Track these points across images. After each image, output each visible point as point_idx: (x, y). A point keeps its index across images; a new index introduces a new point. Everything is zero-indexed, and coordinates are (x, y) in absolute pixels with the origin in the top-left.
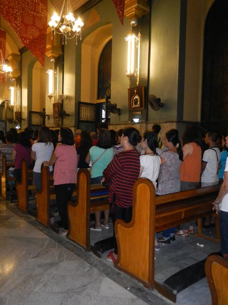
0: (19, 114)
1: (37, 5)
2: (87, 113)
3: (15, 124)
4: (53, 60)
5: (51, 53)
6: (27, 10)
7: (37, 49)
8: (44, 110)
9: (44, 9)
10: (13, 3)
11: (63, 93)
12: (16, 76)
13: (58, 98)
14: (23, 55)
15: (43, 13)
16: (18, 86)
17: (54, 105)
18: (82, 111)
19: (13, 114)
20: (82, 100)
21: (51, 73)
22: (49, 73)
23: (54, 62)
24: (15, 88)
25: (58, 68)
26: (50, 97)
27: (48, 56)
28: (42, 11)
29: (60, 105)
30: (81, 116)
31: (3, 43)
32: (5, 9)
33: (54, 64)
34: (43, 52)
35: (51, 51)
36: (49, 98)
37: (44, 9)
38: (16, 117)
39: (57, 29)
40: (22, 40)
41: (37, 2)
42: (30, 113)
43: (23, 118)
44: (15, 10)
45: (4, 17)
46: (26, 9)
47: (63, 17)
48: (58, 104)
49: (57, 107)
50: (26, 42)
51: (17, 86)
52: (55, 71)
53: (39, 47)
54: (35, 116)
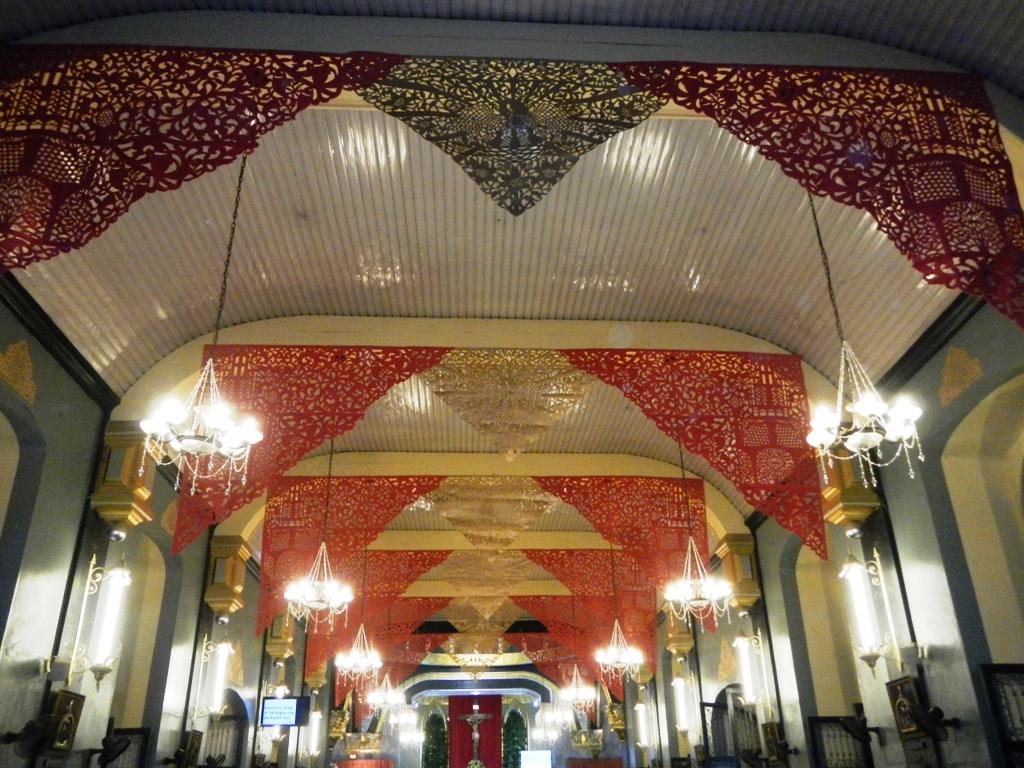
0: (777, 729)
4: (855, 531)
5: (840, 512)
6: (747, 412)
8: (859, 708)
9: (795, 393)
12: (749, 601)
14: (759, 532)
16: (759, 633)
17: (893, 688)
18: (1007, 703)
19: (757, 732)
22: (848, 577)
24: (750, 641)
25: (876, 555)
26: (871, 660)
27: (836, 522)
28: (792, 400)
30: (1010, 725)
32: (689, 427)
33: (859, 541)
34: (815, 513)
35: (841, 505)
36: (865, 664)
37: (795, 393)
38: (768, 742)
39: (838, 449)
40: (746, 495)
41: (771, 382)
42: (813, 723)
45: (688, 448)
46: (745, 409)
47: (849, 408)
49: (904, 696)
50: (758, 498)
51: (756, 634)
52: (868, 566)
54: (831, 732)
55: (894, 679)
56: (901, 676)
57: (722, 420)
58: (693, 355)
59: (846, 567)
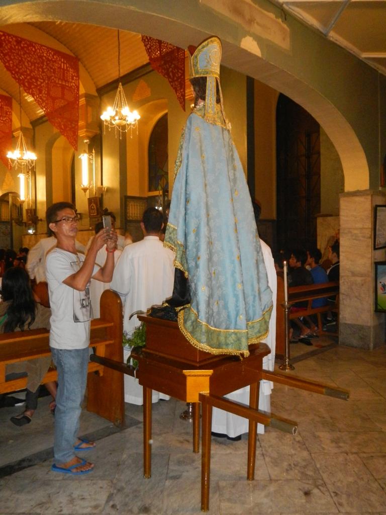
0: (33, 212)
1: (66, 72)
2: (133, 209)
3: (26, 226)
4: (88, 141)
6: (53, 79)
7: (68, 129)
9: (74, 76)
10: (36, 72)
11: (102, 184)
13: (95, 190)
15: (73, 81)
20: (129, 194)
21: (84, 159)
22: (82, 158)
23: (89, 143)
25: (94, 151)
26: (85, 190)
27: (81, 136)
28: (73, 79)
29: (98, 200)
31: (8, 113)
35: (85, 130)
36: (83, 191)
41: (65, 68)
43: (39, 218)
44: (39, 80)
46: (53, 78)
48: (95, 199)
52: (90, 156)
53: (71, 125)
55: (91, 197)
56: (94, 196)
57: (42, 81)
58: (31, 44)
59: (82, 155)
